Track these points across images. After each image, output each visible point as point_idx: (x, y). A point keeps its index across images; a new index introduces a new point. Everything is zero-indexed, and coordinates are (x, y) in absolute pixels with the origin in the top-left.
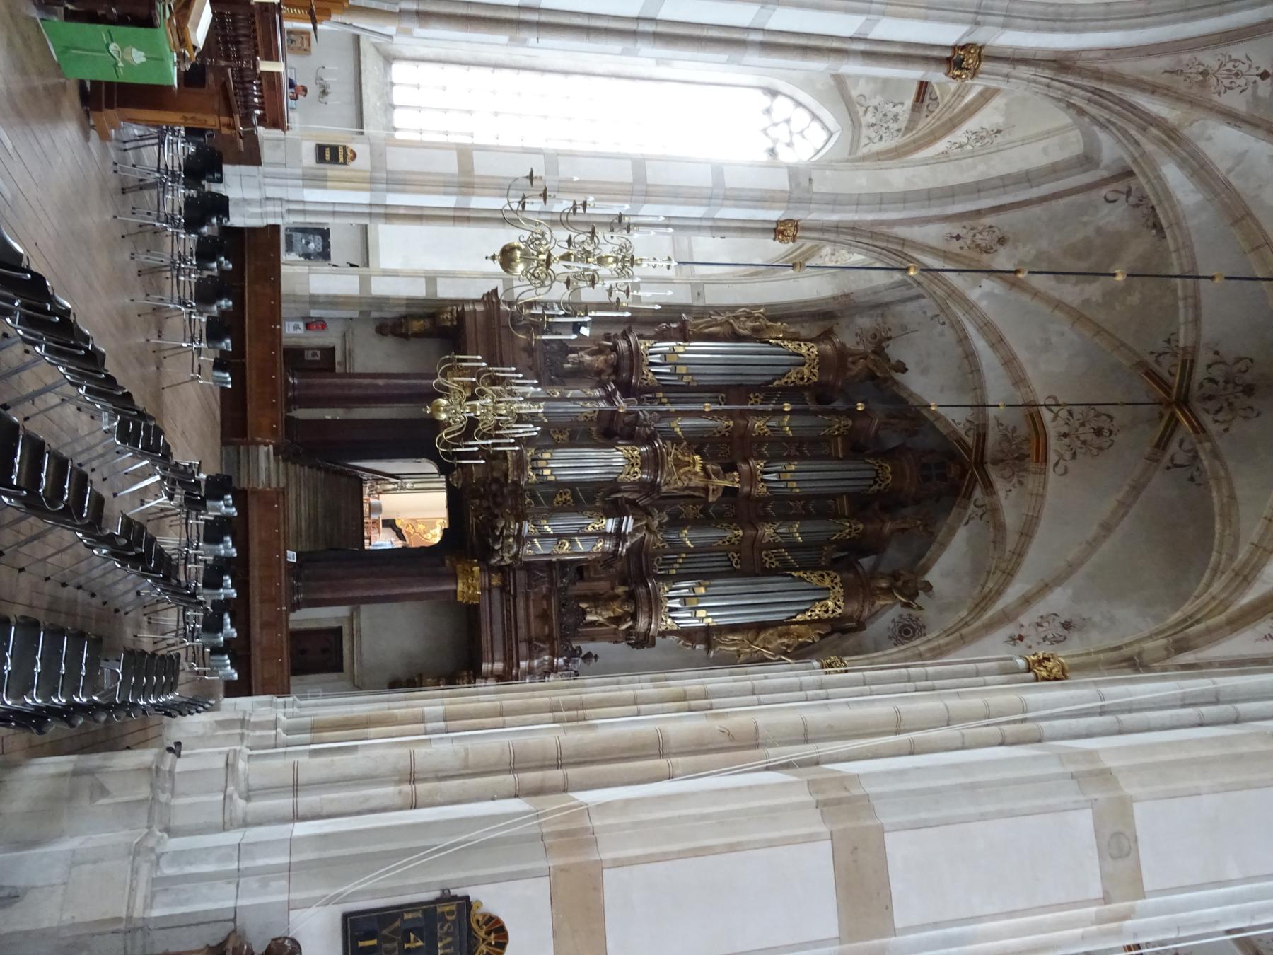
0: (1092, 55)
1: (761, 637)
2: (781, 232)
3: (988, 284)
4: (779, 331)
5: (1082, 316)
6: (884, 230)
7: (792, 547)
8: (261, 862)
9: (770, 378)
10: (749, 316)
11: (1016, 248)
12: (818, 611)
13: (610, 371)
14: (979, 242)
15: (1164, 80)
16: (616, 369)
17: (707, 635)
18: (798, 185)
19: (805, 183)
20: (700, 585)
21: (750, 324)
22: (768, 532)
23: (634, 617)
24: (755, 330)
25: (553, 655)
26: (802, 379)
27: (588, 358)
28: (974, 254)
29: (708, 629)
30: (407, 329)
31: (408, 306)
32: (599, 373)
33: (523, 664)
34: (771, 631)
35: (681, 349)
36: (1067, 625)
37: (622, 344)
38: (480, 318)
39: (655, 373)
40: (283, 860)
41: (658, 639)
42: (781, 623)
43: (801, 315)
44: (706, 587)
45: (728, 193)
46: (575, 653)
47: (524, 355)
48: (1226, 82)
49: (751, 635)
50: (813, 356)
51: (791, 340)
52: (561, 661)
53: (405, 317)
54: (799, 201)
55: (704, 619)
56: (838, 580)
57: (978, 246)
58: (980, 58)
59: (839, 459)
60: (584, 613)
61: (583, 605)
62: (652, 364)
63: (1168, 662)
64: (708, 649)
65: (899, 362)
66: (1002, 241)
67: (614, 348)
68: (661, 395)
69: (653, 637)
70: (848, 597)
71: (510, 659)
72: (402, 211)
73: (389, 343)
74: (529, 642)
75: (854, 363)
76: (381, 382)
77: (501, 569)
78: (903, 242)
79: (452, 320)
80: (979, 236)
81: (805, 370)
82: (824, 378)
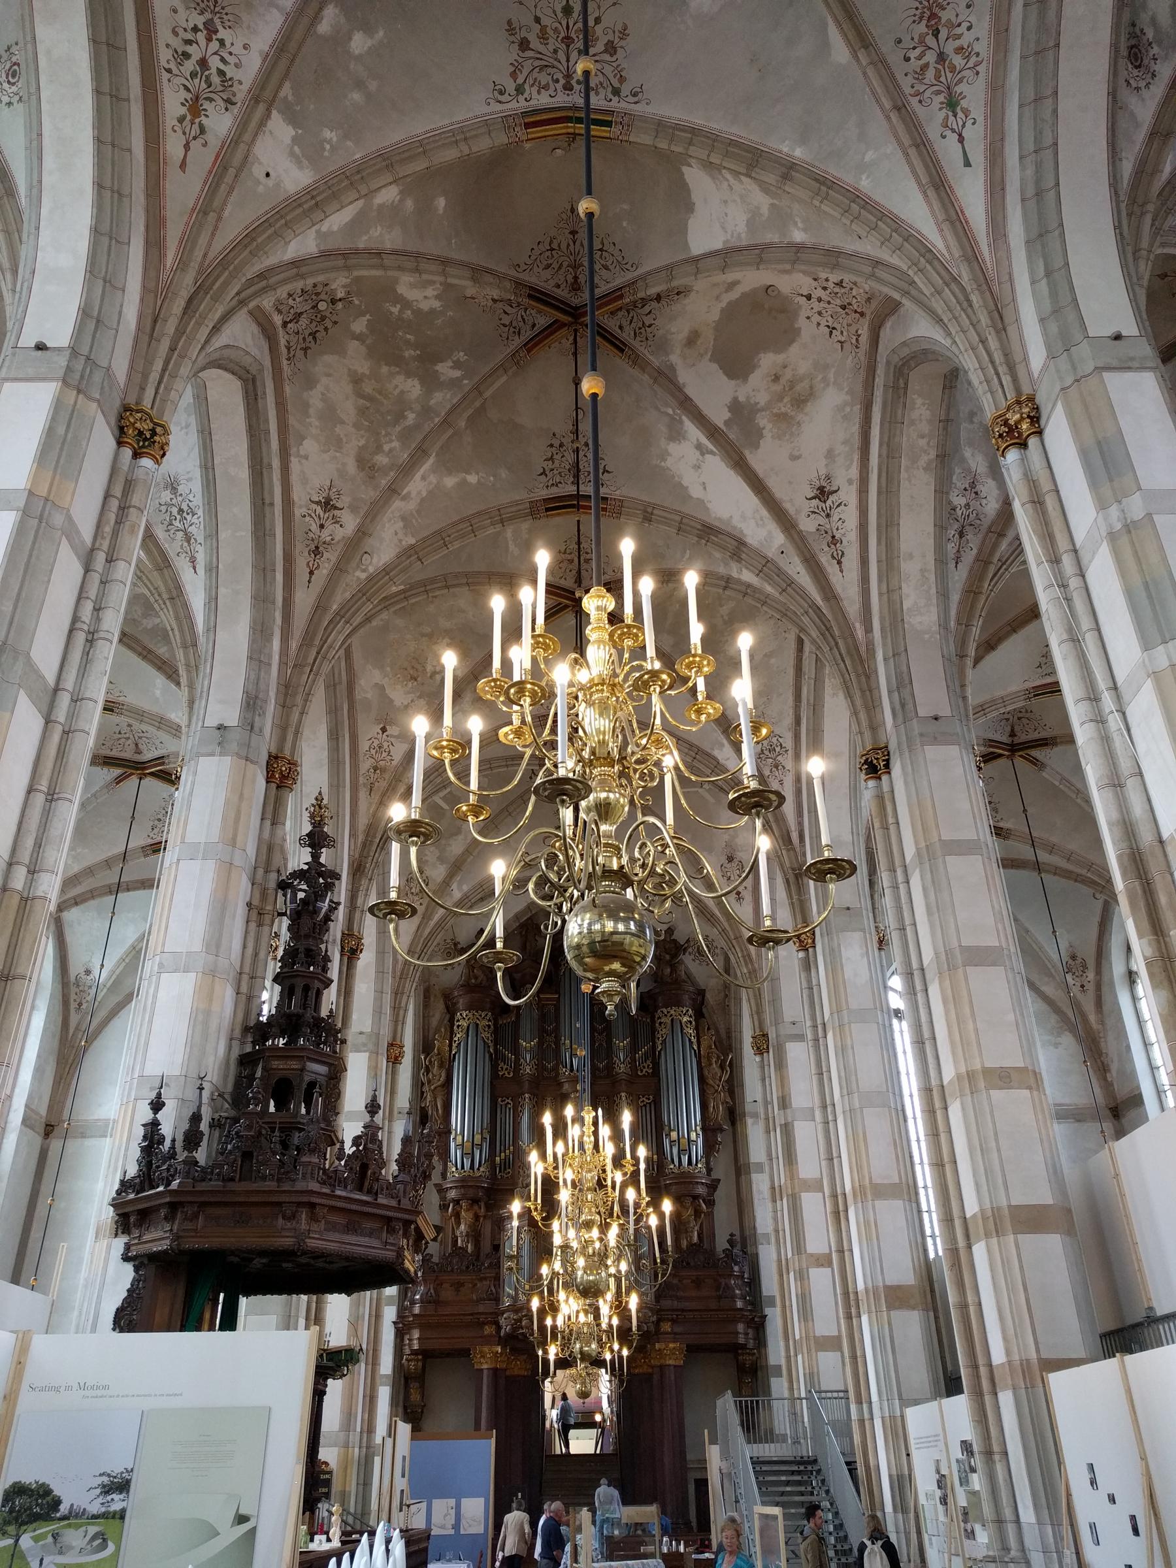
1: (711, 1082)
2: (396, 1058)
3: (454, 886)
7: (634, 1048)
8: (1051, 1540)
9: (487, 1056)
10: (428, 1070)
12: (691, 1031)
13: (476, 1207)
16: (475, 1201)
17: (710, 1130)
18: (365, 1045)
19: (363, 1039)
20: (668, 1135)
22: (622, 1068)
23: (695, 1197)
24: (441, 1066)
25: (731, 1276)
26: (489, 1026)
27: (462, 1227)
29: (702, 1129)
32: (477, 1217)
33: (739, 1304)
34: (706, 1072)
35: (459, 1138)
36: (730, 859)
37: (452, 1194)
39: (480, 1165)
40: (1049, 1529)
41: (714, 1176)
42: (699, 1063)
44: (670, 1130)
46: (728, 1254)
48: (384, 754)
49: (710, 1091)
50: (470, 1015)
51: (452, 1033)
52: (736, 1268)
54: (377, 1045)
55: (697, 1136)
56: (665, 1011)
58: (351, 935)
60: (691, 1245)
61: (684, 1244)
62: (472, 1167)
63: (798, 850)
64: (722, 1130)
67: (457, 1202)
68: (498, 1159)
69: (713, 1180)
70: (679, 1004)
71: (735, 1316)
74: (719, 1298)
75: (476, 978)
77: (659, 1321)
79: (418, 1360)
81: (483, 1023)
82: (488, 1006)
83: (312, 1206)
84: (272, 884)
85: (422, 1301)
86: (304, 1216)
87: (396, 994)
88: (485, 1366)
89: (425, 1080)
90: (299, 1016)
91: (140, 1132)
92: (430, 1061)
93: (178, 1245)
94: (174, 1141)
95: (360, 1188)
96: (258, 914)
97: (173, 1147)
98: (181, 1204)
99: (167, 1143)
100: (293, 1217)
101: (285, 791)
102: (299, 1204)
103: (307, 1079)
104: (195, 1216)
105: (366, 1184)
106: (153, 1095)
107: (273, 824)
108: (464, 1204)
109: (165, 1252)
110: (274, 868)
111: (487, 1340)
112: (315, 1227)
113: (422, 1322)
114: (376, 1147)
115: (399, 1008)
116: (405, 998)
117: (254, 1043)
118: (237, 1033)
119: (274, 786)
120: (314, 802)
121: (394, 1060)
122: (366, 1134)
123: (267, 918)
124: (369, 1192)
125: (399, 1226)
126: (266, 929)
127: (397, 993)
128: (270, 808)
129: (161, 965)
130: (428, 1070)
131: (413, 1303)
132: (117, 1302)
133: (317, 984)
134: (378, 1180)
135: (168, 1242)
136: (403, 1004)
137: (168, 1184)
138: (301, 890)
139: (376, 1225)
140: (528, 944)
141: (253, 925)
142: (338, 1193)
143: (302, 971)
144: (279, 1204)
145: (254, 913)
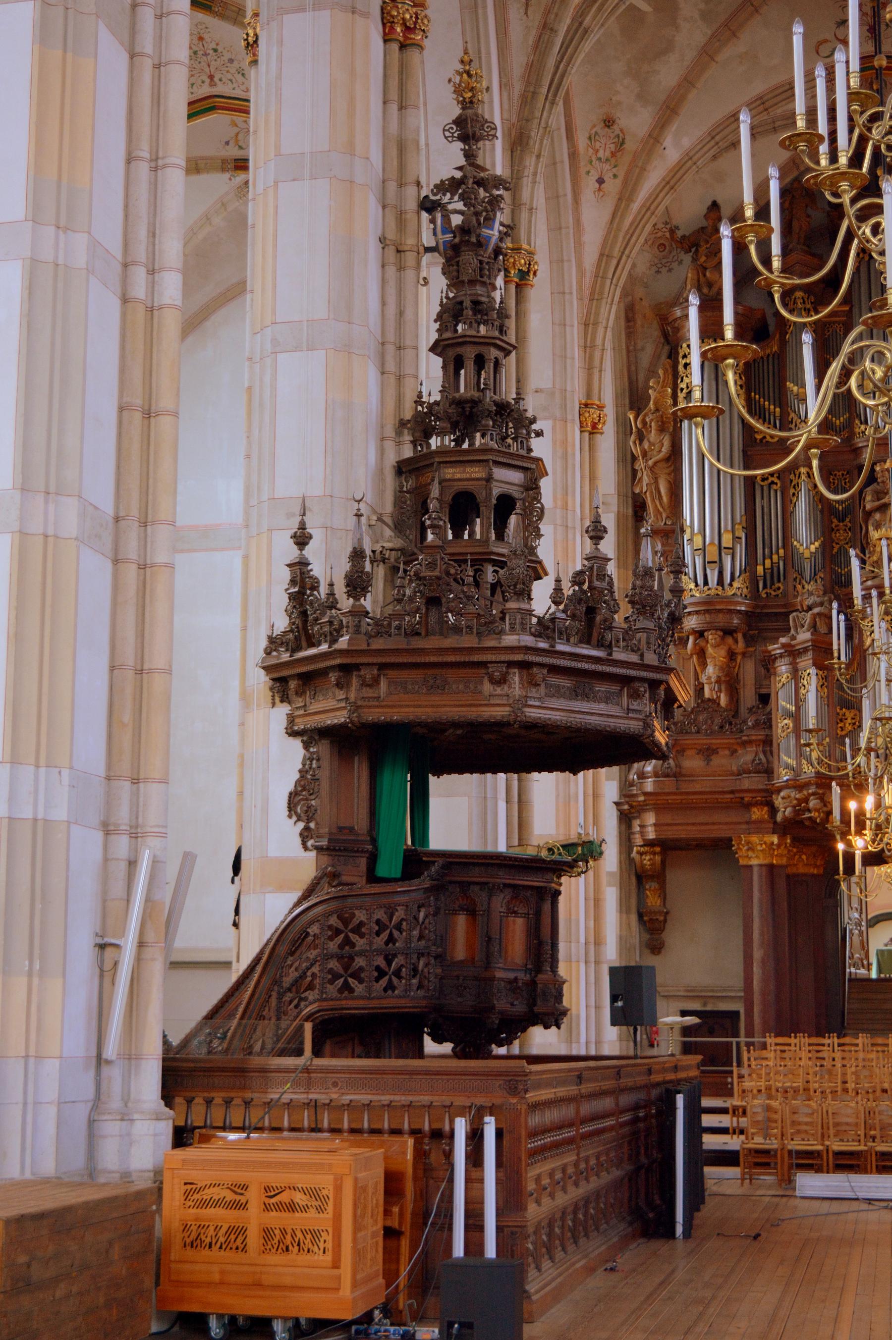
0: (506, 106)
2: (594, 426)
3: (668, 141)
4: (662, 393)
5: (726, 24)
6: (588, 281)
10: (641, 438)
11: (619, 103)
13: (730, 640)
14: (608, 154)
15: (536, 17)
21: (653, 436)
24: (662, 429)
28: (625, 160)
30: (660, 913)
31: (628, 912)
32: (731, 655)
38: (668, 818)
39: (733, 579)
43: (628, 351)
45: (559, 503)
47: (716, 761)
53: (640, 916)
54: (564, 407)
57: (613, 154)
59: (851, 309)
62: (720, 582)
65: (706, 216)
66: (609, 123)
67: (700, 634)
68: (760, 569)
72: (592, 923)
73: (673, 938)
76: (758, 954)
78: (604, 256)
79: (654, 854)
80: (601, 154)
83: (524, 666)
84: (412, 204)
85: (656, 775)
86: (517, 679)
87: (586, 325)
88: (754, 862)
89: (637, 451)
90: (474, 403)
91: (286, 575)
92: (644, 423)
93: (359, 717)
94: (331, 585)
95: (586, 639)
96: (396, 251)
97: (331, 594)
98: (357, 667)
99: (323, 590)
100: (503, 680)
101: (414, 55)
102: (510, 664)
103: (496, 492)
104: (376, 682)
105: (595, 634)
106: (294, 525)
107: (401, 108)
108: (710, 636)
109: (342, 727)
110: (411, 178)
111: (756, 827)
112: (533, 692)
113: (659, 803)
114: (605, 585)
115: (593, 346)
116: (601, 330)
117: (414, 443)
118: (390, 431)
119: (395, 46)
120: (460, 67)
121: (593, 430)
122: (591, 569)
123: (410, 258)
124: (600, 645)
125: (643, 688)
126: (410, 274)
127: (588, 324)
128: (394, 83)
129: (274, 341)
130: (641, 438)
131: (642, 776)
132: (290, 787)
133: (494, 353)
134: (610, 628)
135: (345, 713)
136: (599, 341)
137: (334, 641)
138: (457, 212)
139: (615, 688)
140: (795, 224)
141: (391, 271)
142: (560, 647)
143: (474, 334)
144: (484, 664)
145: (391, 252)
